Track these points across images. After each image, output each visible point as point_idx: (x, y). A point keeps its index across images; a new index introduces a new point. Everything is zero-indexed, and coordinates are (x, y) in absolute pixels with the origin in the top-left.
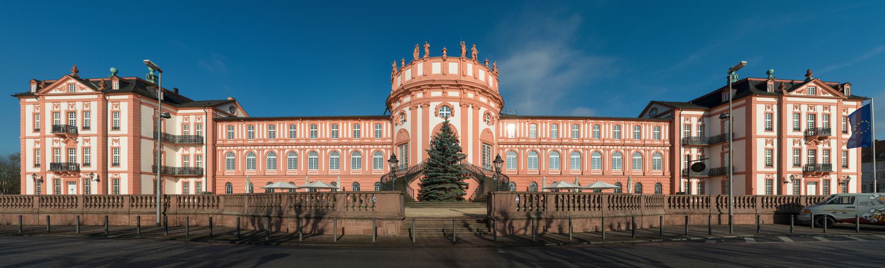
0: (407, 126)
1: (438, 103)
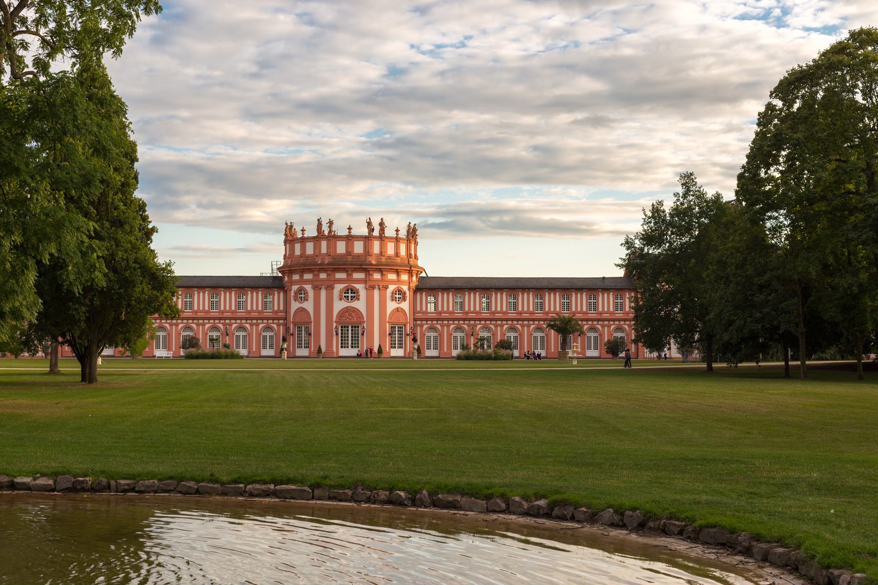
0: (309, 306)
1: (342, 286)
